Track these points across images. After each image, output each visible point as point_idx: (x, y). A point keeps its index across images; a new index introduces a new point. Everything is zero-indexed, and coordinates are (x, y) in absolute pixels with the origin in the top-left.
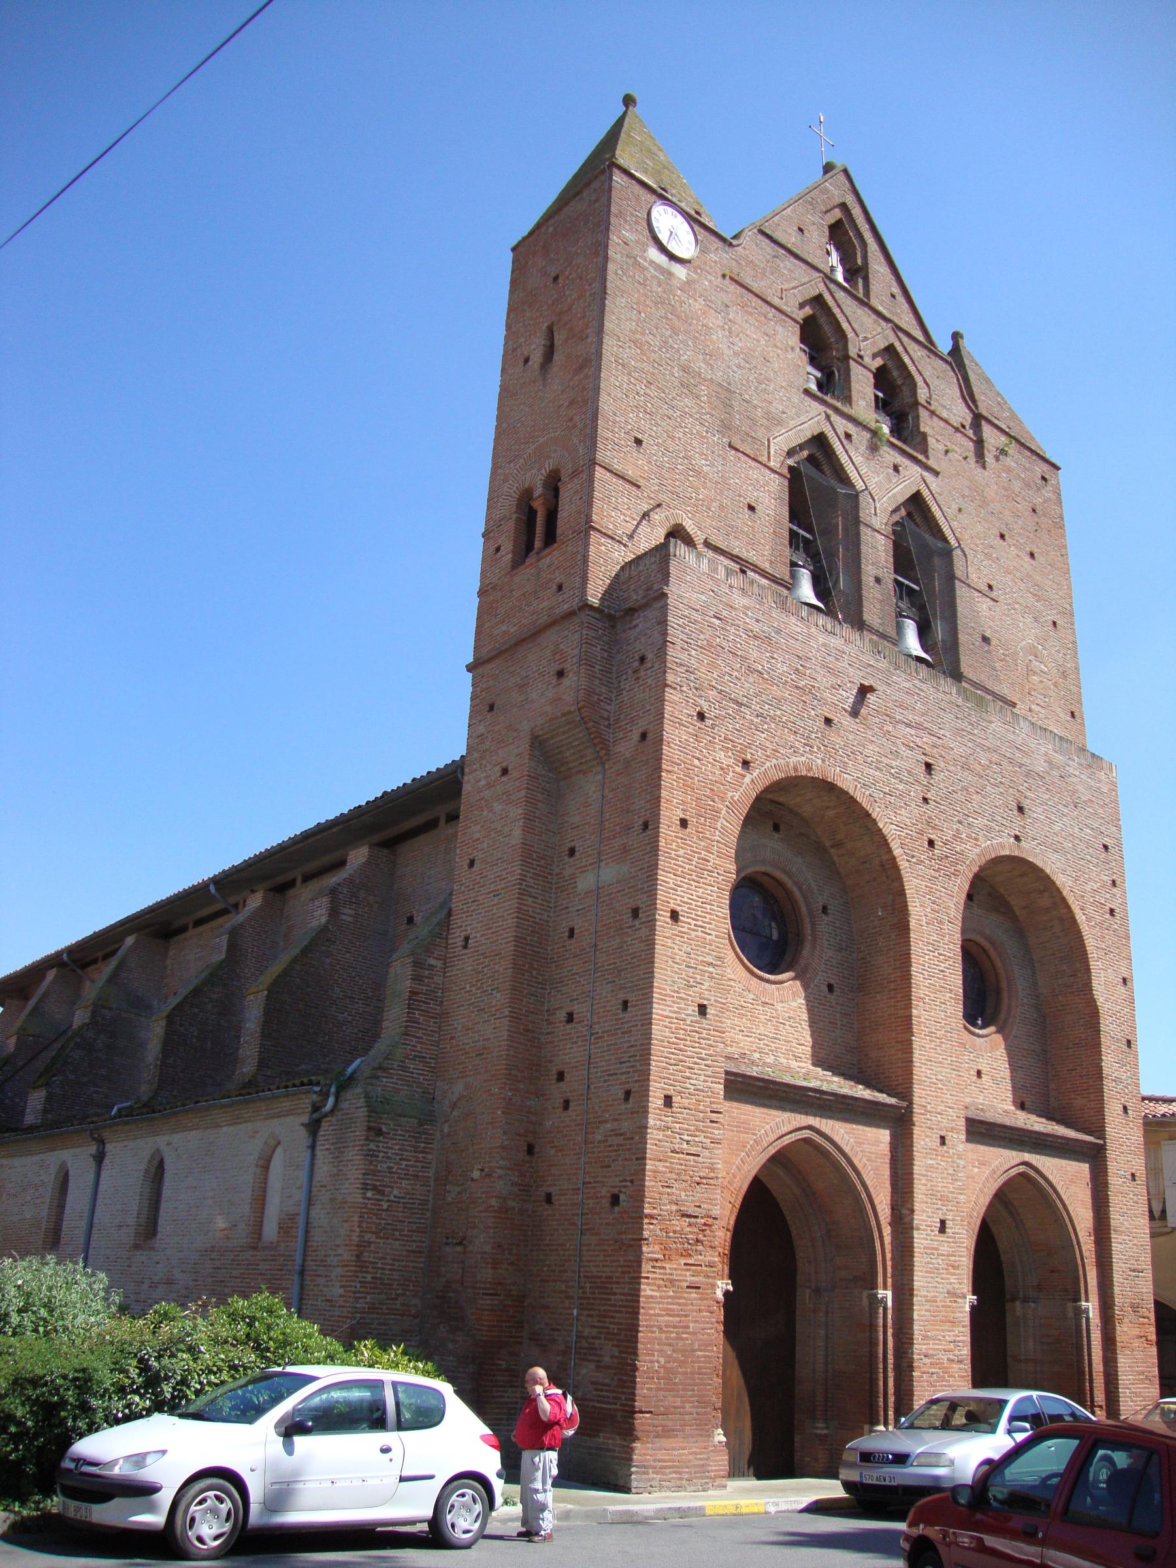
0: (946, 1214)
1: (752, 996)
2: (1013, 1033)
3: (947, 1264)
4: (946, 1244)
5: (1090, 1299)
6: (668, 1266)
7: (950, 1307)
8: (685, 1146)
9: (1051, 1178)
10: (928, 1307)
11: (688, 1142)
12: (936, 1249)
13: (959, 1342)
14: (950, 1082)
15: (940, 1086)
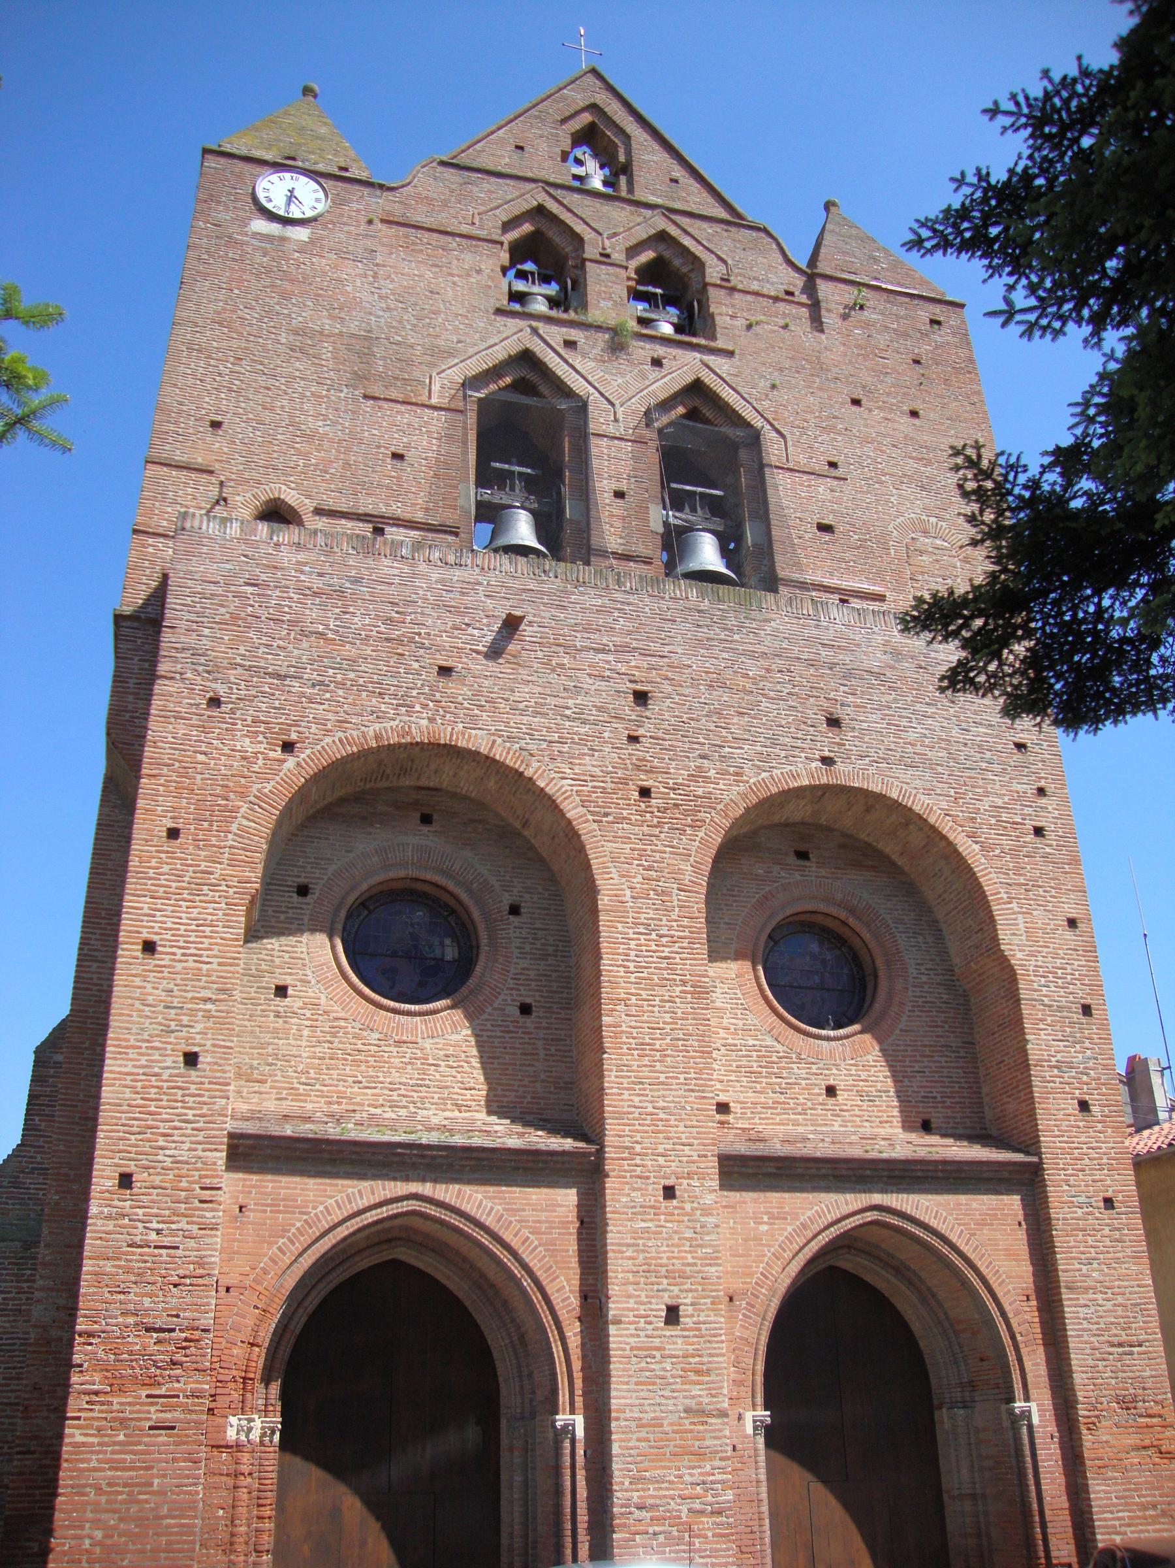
0: (678, 1297)
1: (377, 1036)
2: (902, 1026)
3: (683, 1370)
4: (679, 1341)
5: (1032, 1397)
6: (115, 1400)
7: (691, 1431)
8: (153, 1236)
9: (933, 1223)
10: (643, 1435)
11: (159, 1232)
12: (658, 1349)
13: (713, 1482)
14: (684, 1108)
15: (662, 1116)
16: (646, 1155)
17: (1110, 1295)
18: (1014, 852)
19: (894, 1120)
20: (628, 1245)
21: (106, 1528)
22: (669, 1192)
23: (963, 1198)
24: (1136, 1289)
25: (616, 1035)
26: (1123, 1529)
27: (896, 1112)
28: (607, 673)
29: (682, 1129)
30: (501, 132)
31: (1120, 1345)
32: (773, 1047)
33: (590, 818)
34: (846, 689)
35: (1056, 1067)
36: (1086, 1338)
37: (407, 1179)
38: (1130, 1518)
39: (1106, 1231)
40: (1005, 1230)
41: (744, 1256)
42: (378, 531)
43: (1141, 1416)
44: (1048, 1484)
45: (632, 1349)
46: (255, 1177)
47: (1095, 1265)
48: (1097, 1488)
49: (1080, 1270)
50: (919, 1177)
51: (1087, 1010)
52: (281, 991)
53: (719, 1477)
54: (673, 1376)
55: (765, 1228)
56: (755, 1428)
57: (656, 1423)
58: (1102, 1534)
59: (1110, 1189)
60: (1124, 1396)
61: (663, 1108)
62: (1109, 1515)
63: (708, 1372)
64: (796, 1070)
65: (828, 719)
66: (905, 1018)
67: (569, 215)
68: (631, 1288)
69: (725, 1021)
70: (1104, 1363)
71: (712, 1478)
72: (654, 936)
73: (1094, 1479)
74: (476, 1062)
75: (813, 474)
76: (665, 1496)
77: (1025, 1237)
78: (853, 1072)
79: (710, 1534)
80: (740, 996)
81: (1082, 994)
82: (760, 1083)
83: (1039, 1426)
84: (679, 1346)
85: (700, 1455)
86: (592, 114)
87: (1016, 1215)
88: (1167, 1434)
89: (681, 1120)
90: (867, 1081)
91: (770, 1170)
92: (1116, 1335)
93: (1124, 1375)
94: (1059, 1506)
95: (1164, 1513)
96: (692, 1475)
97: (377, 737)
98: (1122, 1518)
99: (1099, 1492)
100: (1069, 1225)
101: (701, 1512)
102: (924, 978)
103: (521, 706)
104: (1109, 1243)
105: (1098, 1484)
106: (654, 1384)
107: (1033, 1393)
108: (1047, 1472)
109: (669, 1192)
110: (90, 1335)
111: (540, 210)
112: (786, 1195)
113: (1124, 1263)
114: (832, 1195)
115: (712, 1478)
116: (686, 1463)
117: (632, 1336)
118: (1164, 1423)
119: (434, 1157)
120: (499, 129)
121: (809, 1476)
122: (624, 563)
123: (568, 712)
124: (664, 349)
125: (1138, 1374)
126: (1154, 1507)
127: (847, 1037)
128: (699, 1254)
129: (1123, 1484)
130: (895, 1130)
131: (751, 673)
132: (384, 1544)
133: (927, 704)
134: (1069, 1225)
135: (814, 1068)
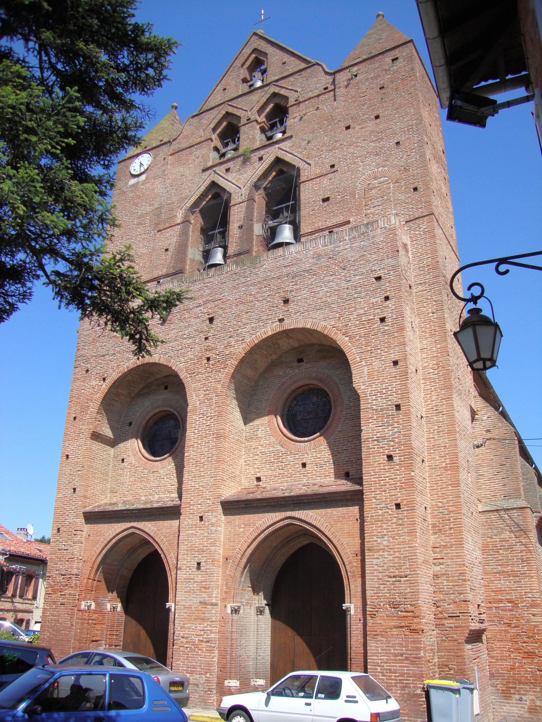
0: (200, 559)
1: (147, 471)
2: (339, 429)
3: (200, 587)
4: (200, 576)
5: (352, 601)
6: (53, 596)
7: (201, 610)
8: (63, 546)
9: (314, 523)
10: (185, 611)
11: (65, 545)
12: (192, 579)
13: (207, 630)
14: (209, 485)
15: (201, 489)
16: (194, 505)
17: (392, 553)
18: (366, 336)
19: (331, 474)
20: (186, 540)
21: (50, 633)
22: (201, 518)
23: (329, 510)
24: (407, 549)
25: (189, 459)
26: (382, 664)
27: (332, 471)
28: (200, 315)
29: (207, 493)
30: (218, 88)
31: (394, 577)
32: (280, 450)
33: (188, 376)
34: (293, 283)
35: (375, 440)
36: (375, 574)
37: (130, 522)
38: (387, 659)
39: (395, 520)
40: (349, 523)
41: (233, 542)
42: (159, 282)
43: (402, 612)
44: (354, 641)
45: (184, 579)
46: (92, 525)
47: (386, 538)
48: (372, 645)
49: (377, 541)
50: (306, 503)
51: (398, 407)
52: (123, 460)
53: (209, 628)
54: (197, 590)
55: (242, 530)
56: (232, 611)
57: (190, 607)
58: (371, 666)
59: (399, 499)
60: (393, 602)
61: (202, 486)
62: (376, 658)
63: (208, 588)
64: (289, 459)
65: (284, 301)
66: (341, 425)
67: (284, 90)
68: (185, 556)
69: (262, 443)
70: (384, 586)
71: (207, 628)
72: (205, 418)
73: (370, 640)
74: (175, 475)
75: (322, 176)
76: (191, 634)
77: (359, 526)
78: (314, 455)
79: (204, 649)
80: (268, 430)
81: (395, 400)
82: (274, 466)
83: (354, 615)
84: (199, 578)
85: (203, 619)
86: (255, 54)
87: (355, 516)
88: (415, 620)
89: (207, 490)
90: (320, 458)
91: (243, 506)
92: (392, 572)
93: (394, 591)
94: (359, 652)
95: (407, 659)
96: (200, 627)
97: (127, 367)
98: (383, 659)
99: (372, 646)
100: (373, 519)
101: (202, 641)
102: (352, 404)
103: (170, 339)
104: (395, 527)
105: (372, 643)
106: (190, 592)
107: (353, 600)
108: (354, 636)
109: (201, 518)
110: (49, 577)
111: (228, 114)
112: (252, 516)
113: (402, 536)
114: (270, 514)
115: (207, 628)
116: (199, 622)
117: (184, 574)
118: (415, 615)
119: (135, 513)
120: (217, 86)
121: (295, 633)
122: (239, 257)
123: (185, 336)
124: (264, 151)
125: (402, 591)
126: (402, 655)
127: (314, 439)
128: (209, 542)
129: (386, 643)
130: (331, 479)
131: (253, 293)
132: (152, 647)
133: (331, 275)
134: (373, 519)
135: (297, 456)
